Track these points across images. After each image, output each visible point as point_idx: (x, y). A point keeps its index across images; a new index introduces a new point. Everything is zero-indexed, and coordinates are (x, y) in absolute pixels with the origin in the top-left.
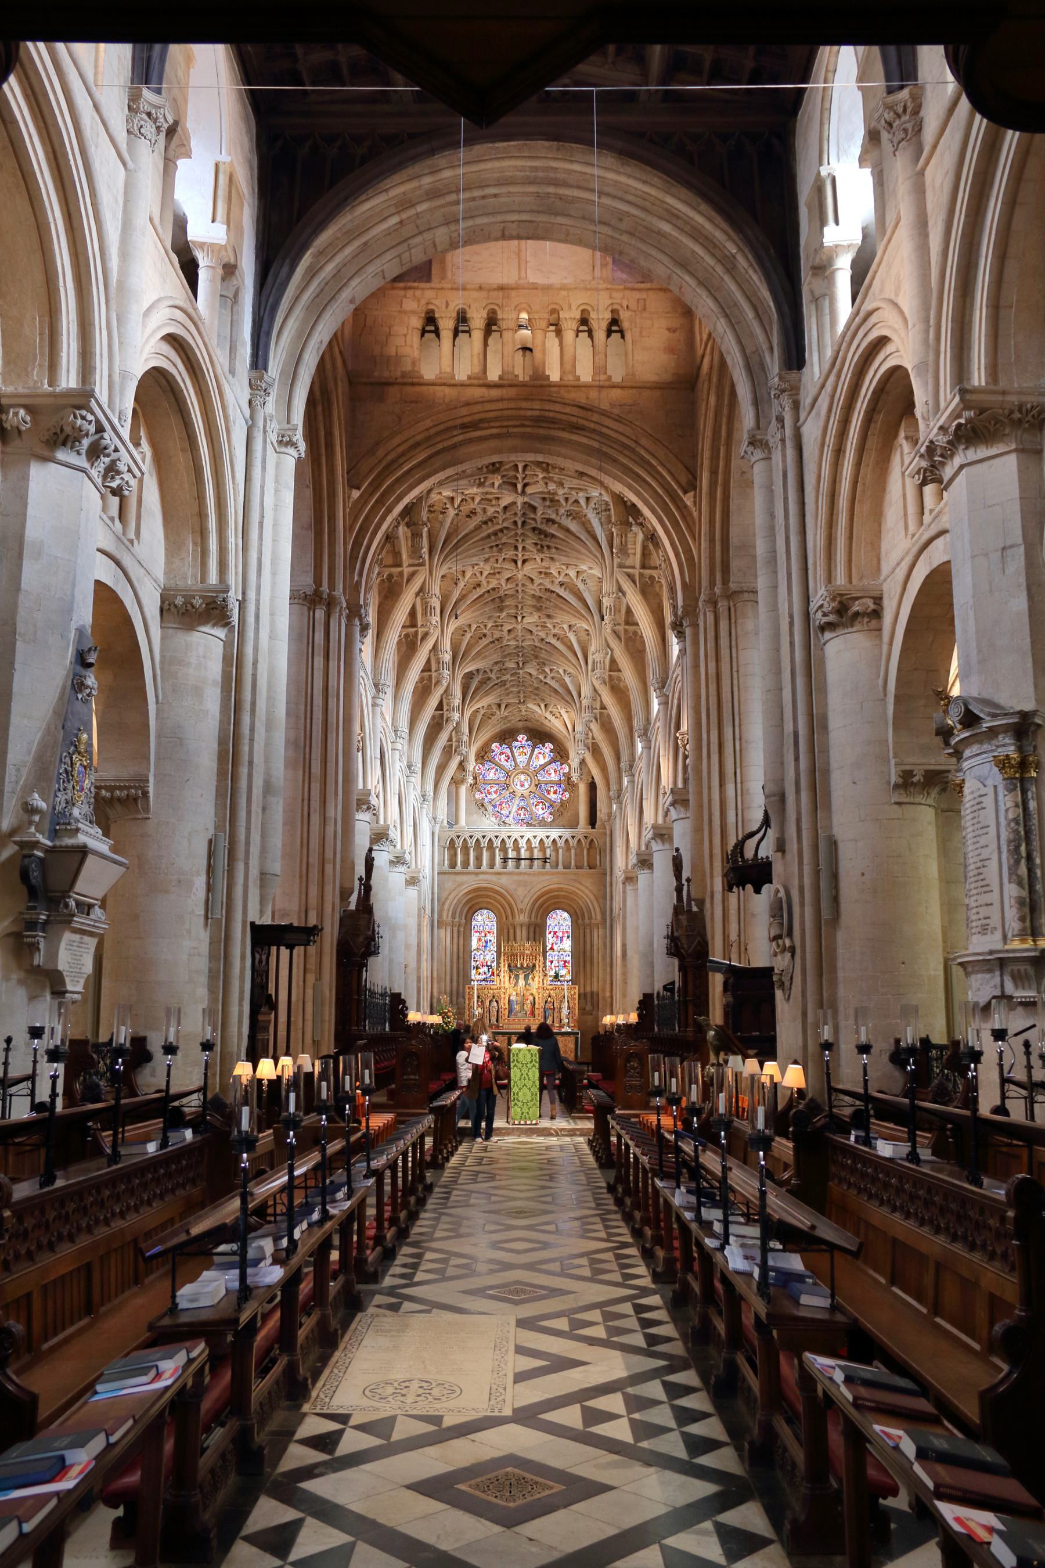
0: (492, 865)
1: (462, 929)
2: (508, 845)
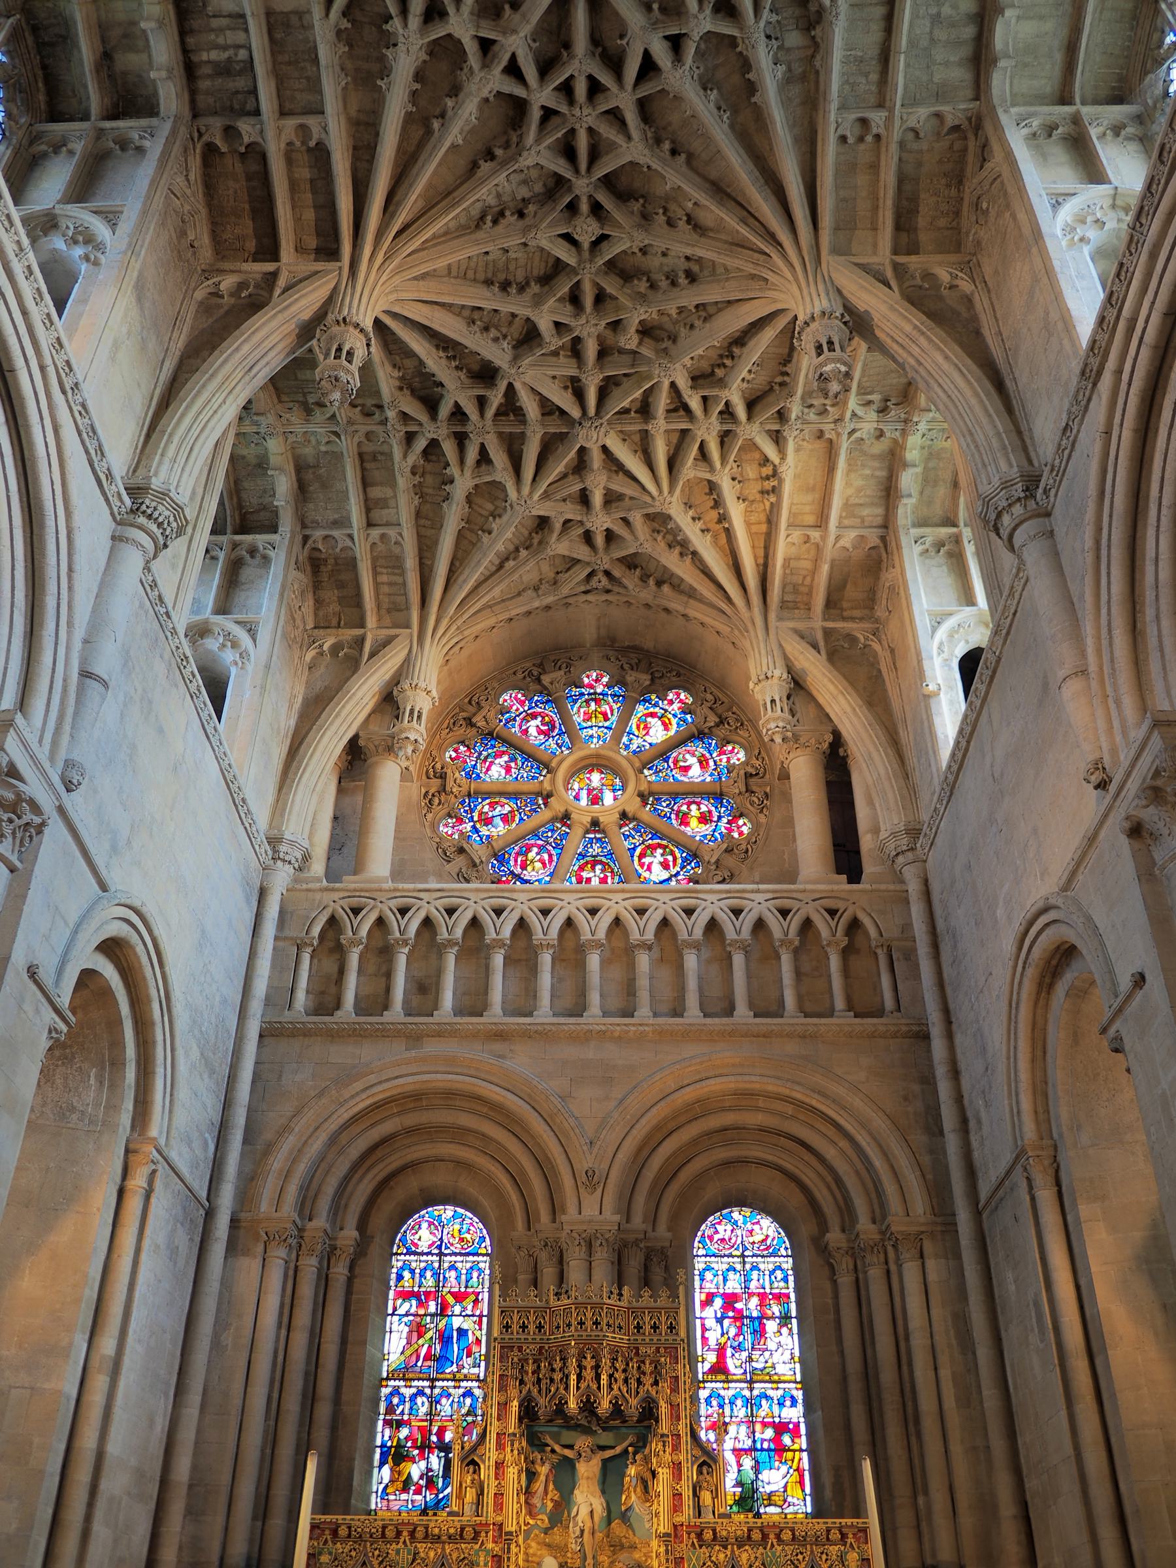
1: (340, 1271)
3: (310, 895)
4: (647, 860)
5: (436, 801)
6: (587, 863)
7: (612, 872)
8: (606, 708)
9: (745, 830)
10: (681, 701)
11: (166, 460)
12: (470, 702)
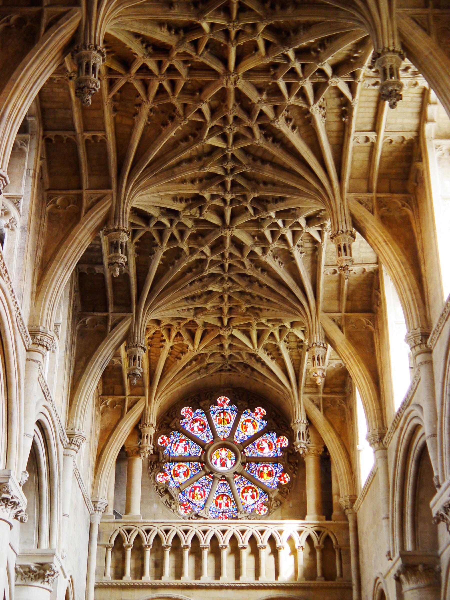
0: (179, 573)
2: (202, 544)
3: (110, 524)
4: (245, 494)
5: (155, 466)
6: (220, 495)
7: (231, 500)
8: (228, 417)
9: (287, 480)
10: (261, 414)
11: (78, 418)
12: (168, 415)
